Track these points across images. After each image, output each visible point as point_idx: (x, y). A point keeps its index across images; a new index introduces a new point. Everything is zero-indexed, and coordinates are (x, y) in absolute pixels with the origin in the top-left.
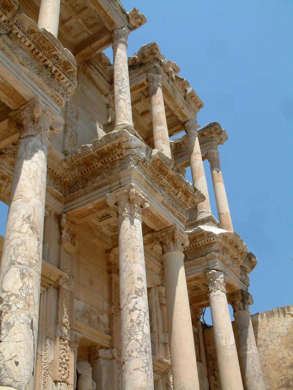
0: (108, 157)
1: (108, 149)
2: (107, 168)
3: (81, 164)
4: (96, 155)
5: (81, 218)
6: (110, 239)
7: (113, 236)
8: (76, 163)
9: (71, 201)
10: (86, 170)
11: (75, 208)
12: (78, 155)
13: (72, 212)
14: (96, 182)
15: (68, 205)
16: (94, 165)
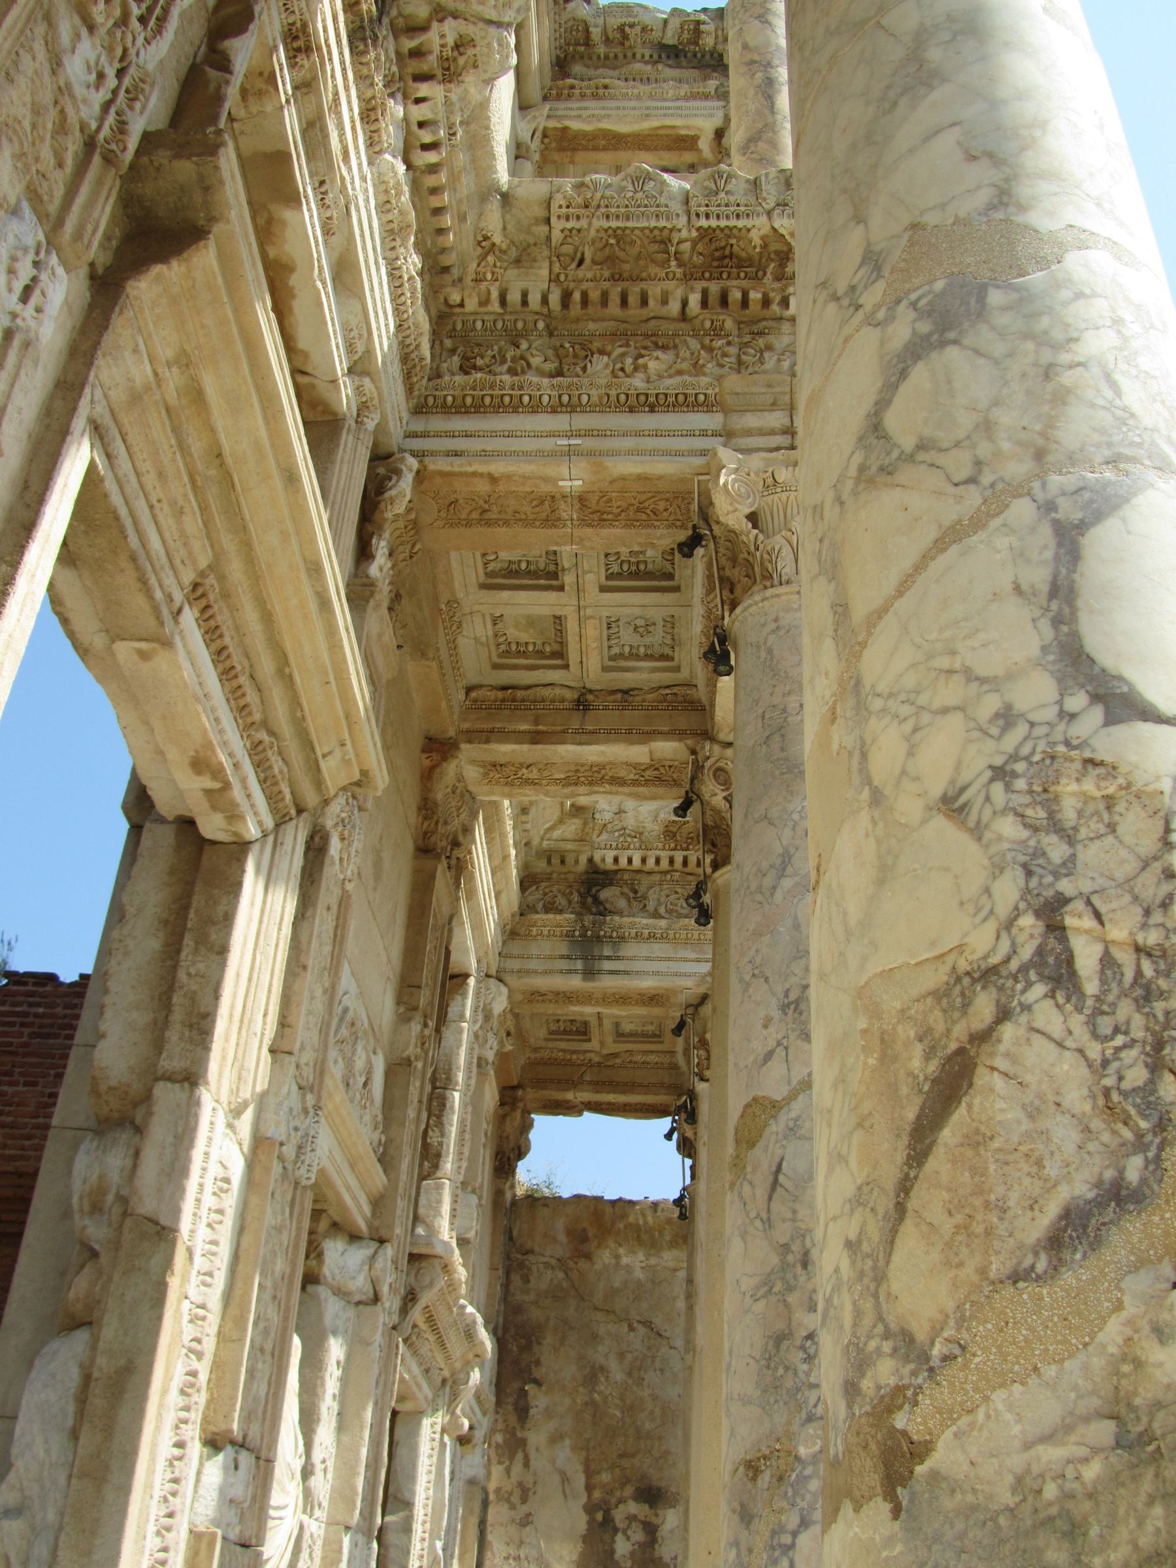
0: (745, 283)
1: (765, 246)
2: (717, 331)
3: (579, 255)
4: (686, 247)
5: (469, 524)
6: (461, 696)
7: (480, 686)
8: (557, 236)
9: (461, 408)
10: (594, 295)
11: (484, 454)
12: (594, 203)
13: (456, 465)
14: (640, 375)
15: (438, 423)
16: (655, 291)
